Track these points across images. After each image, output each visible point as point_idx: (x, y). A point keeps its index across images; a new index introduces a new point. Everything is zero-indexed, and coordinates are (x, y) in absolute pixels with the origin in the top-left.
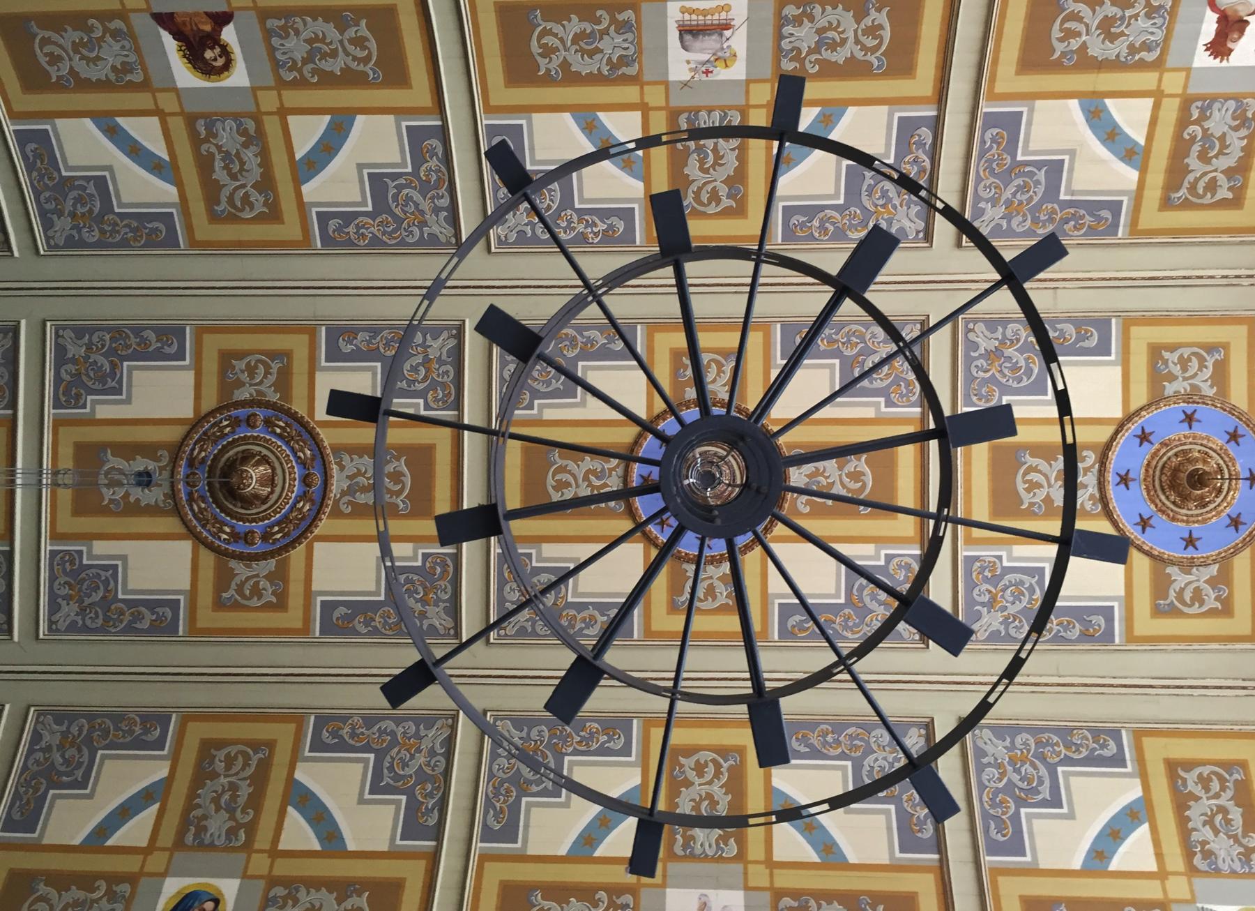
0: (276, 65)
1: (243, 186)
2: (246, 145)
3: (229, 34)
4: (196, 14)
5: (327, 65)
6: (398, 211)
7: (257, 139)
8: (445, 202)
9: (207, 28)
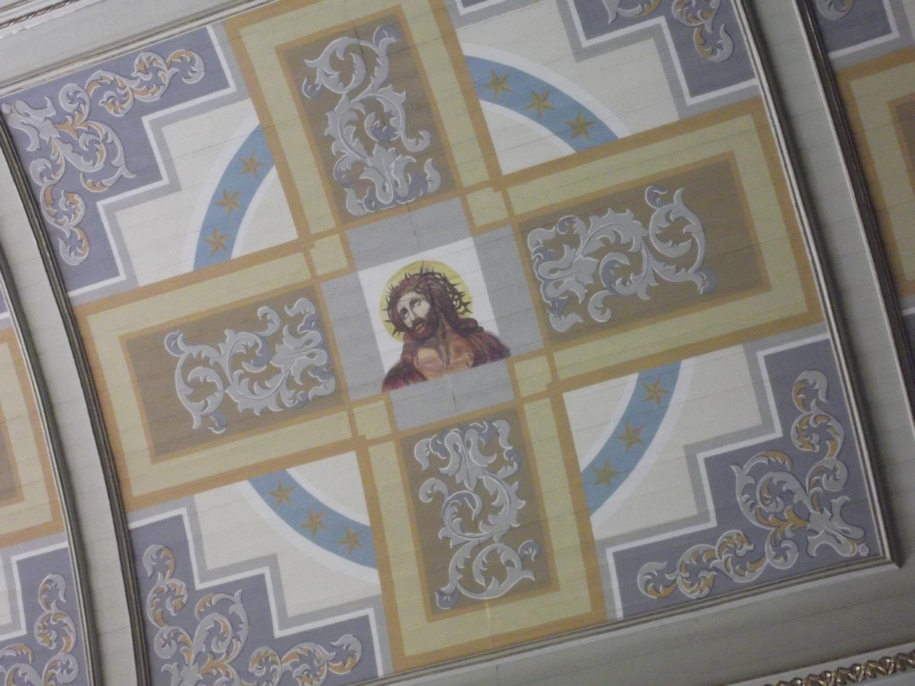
0: (319, 322)
1: (352, 94)
2: (359, 166)
3: (390, 350)
4: (439, 372)
5: (247, 338)
6: (102, 129)
7: (342, 183)
8: (35, 168)
9: (425, 354)
